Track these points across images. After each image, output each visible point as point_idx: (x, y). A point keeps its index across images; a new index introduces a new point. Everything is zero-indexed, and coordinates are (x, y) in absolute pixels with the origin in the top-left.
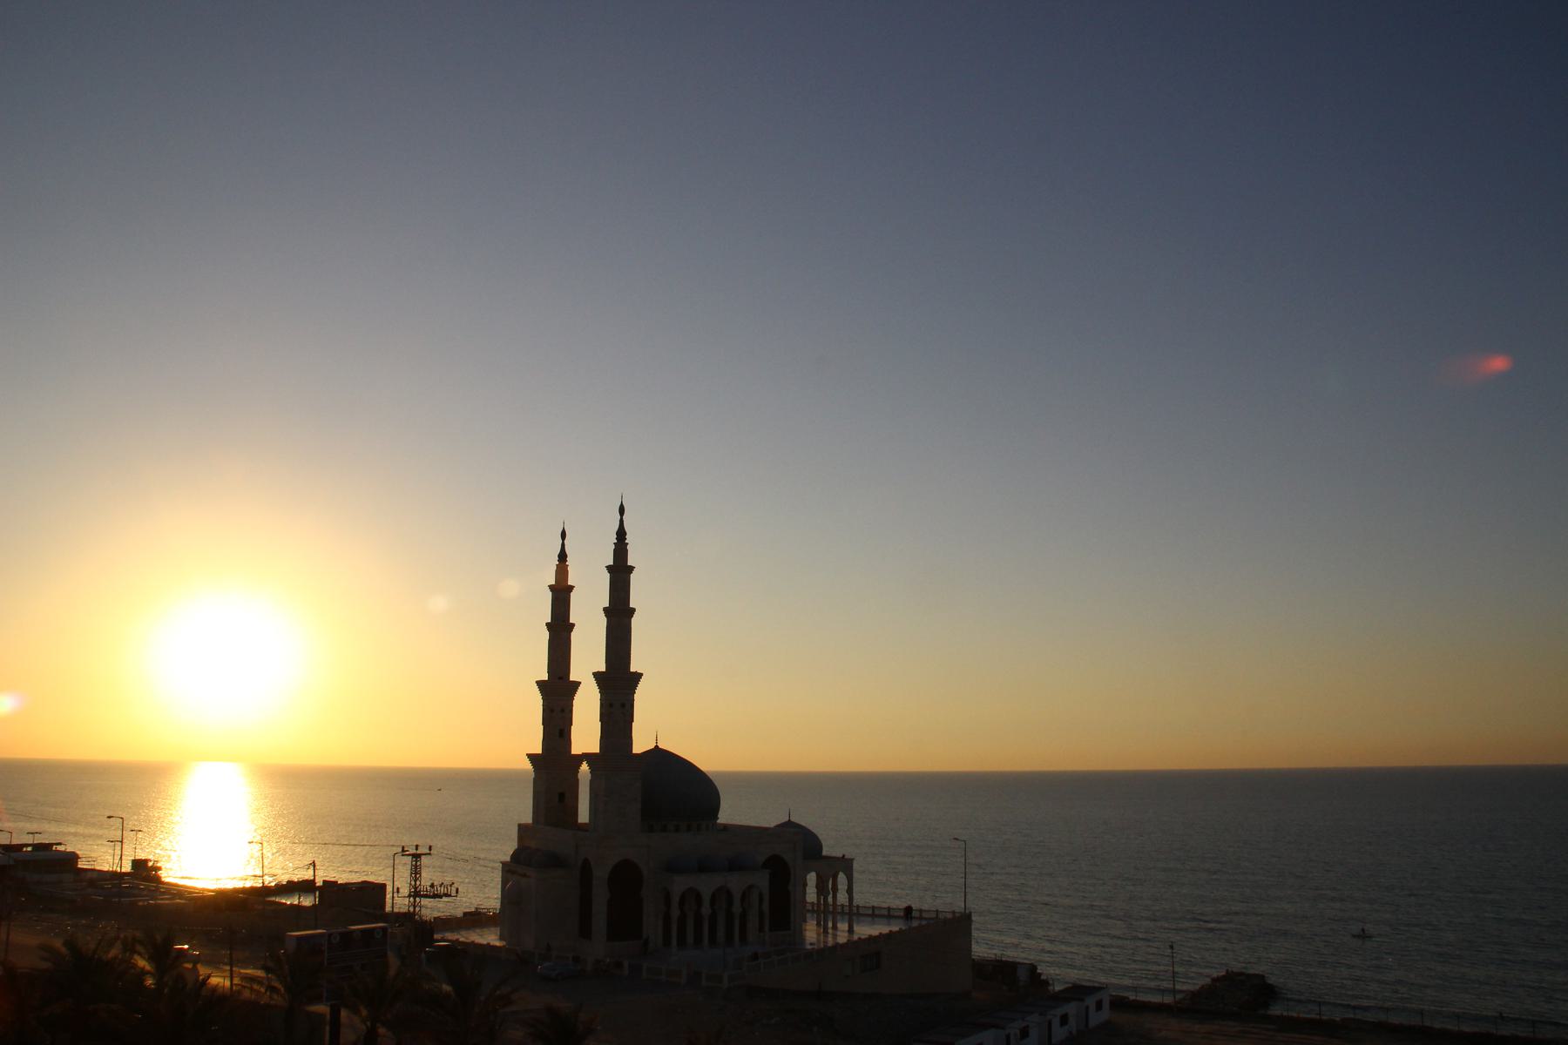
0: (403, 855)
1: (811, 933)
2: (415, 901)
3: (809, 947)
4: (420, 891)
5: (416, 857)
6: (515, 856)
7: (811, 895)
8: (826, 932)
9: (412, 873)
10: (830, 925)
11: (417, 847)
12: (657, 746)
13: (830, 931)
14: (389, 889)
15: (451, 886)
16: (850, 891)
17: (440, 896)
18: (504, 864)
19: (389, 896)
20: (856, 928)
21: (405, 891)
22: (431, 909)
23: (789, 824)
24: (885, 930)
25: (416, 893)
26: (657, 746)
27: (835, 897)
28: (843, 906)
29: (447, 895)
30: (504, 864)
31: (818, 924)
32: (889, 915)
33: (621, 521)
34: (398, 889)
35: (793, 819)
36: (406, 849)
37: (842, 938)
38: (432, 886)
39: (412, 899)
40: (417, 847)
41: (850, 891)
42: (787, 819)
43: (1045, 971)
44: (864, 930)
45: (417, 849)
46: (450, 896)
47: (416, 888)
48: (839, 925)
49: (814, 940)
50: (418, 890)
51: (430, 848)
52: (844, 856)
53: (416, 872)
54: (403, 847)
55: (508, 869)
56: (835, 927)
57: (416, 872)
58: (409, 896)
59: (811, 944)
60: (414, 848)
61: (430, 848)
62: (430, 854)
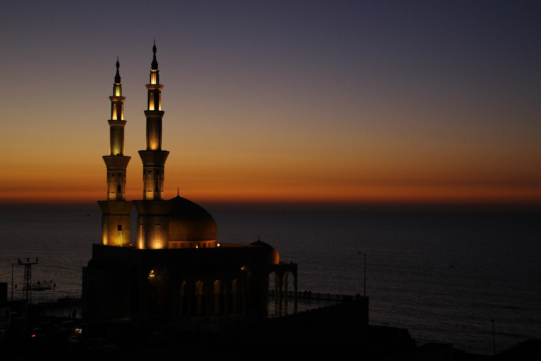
0: (19, 265)
1: (272, 308)
2: (27, 293)
3: (271, 317)
4: (31, 287)
5: (28, 265)
6: (90, 263)
7: (272, 285)
8: (281, 307)
9: (25, 276)
10: (283, 303)
11: (28, 260)
12: (178, 196)
13: (283, 307)
14: (9, 286)
15: (51, 283)
16: (295, 284)
17: (43, 289)
18: (84, 268)
19: (9, 290)
20: (298, 306)
21: (20, 287)
22: (36, 296)
23: (259, 243)
24: (316, 307)
25: (28, 288)
26: (178, 196)
27: (286, 287)
28: (291, 292)
29: (48, 288)
30: (84, 268)
31: (276, 303)
32: (318, 298)
33: (155, 57)
34: (16, 286)
35: (261, 240)
36: (21, 261)
37: (291, 312)
38: (38, 283)
39: (25, 292)
40: (28, 259)
41: (295, 284)
42: (257, 240)
43: (414, 334)
44: (302, 307)
45: (28, 260)
46: (50, 289)
47: (28, 284)
48: (289, 304)
49: (273, 313)
50: (29, 285)
51: (37, 260)
52: (292, 262)
53: (28, 275)
54: (19, 260)
55: (86, 271)
56: (286, 305)
57: (28, 275)
58: (24, 290)
59: (272, 315)
60: (27, 260)
61: (37, 260)
62: (37, 263)
